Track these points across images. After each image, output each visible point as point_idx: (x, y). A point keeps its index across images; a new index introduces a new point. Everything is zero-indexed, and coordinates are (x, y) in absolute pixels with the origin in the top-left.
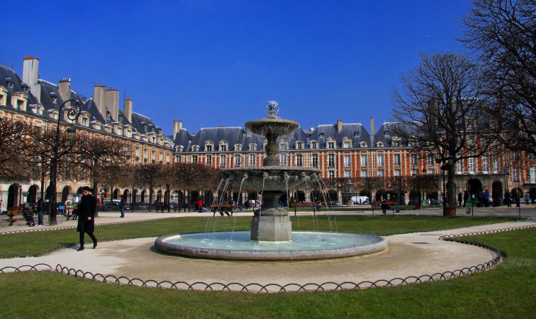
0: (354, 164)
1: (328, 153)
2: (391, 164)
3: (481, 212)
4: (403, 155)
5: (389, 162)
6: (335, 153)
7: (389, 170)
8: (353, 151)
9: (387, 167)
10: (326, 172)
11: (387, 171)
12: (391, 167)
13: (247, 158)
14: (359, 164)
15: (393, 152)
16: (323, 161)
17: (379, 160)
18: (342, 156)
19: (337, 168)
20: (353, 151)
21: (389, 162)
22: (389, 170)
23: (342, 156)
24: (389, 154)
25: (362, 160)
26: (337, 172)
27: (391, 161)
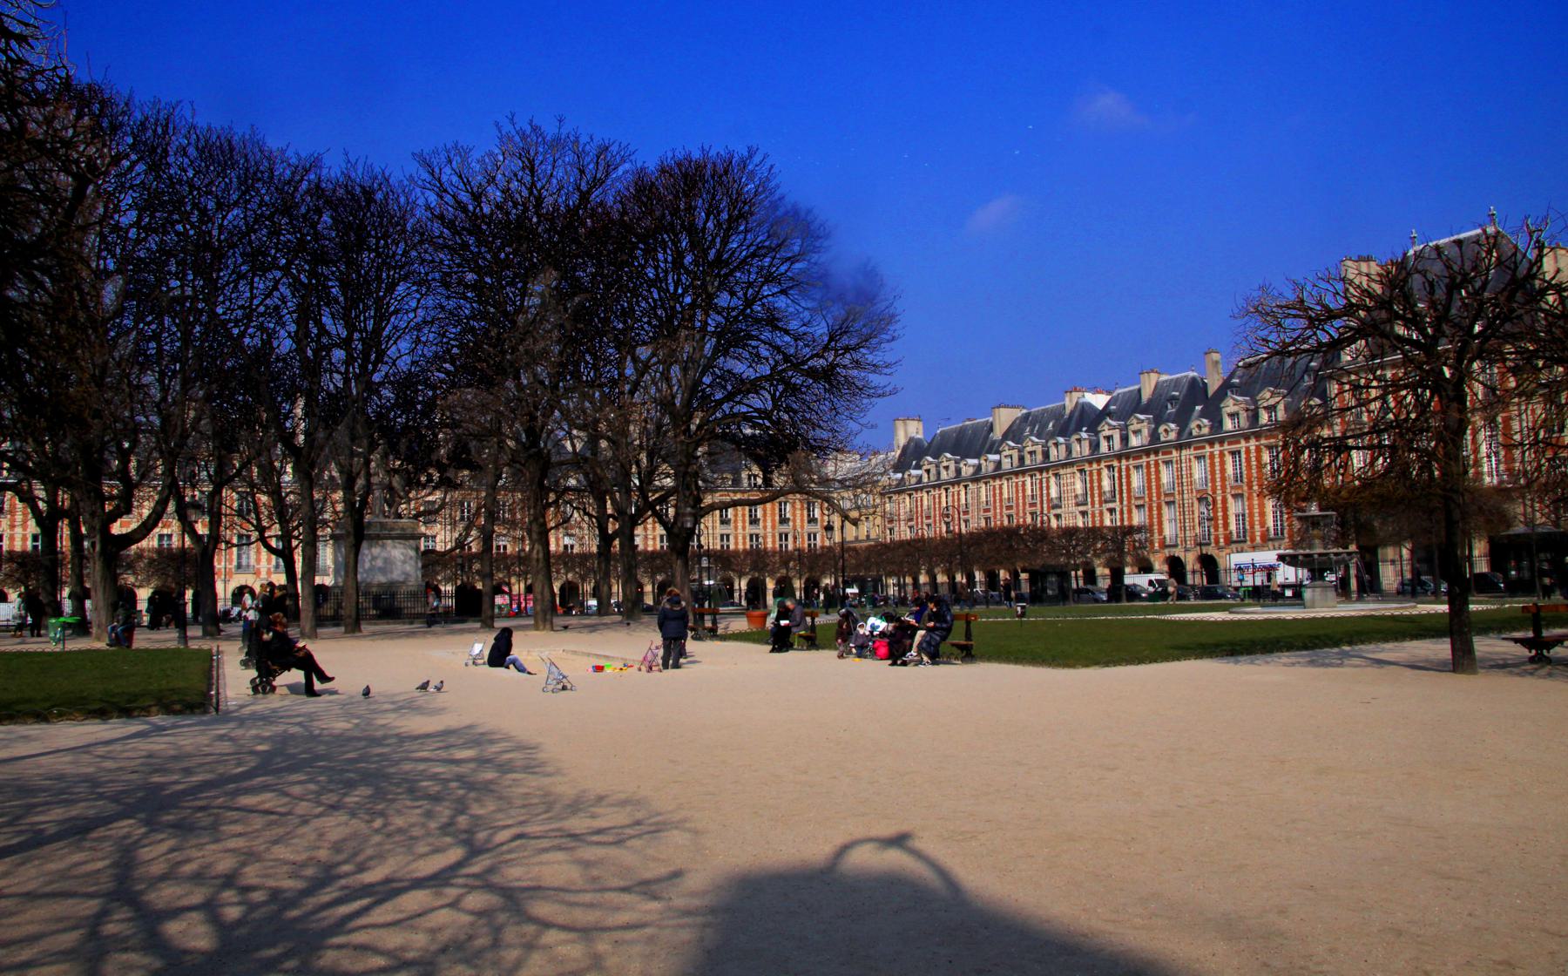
0: (1150, 488)
1: (1103, 465)
2: (1223, 479)
3: (158, 641)
4: (1248, 451)
5: (1218, 476)
6: (1115, 463)
7: (1219, 498)
8: (1247, 439)
9: (1214, 491)
10: (1101, 514)
11: (1214, 501)
12: (1224, 488)
13: (979, 490)
14: (1158, 486)
15: (1226, 446)
17: (1198, 471)
18: (1128, 469)
20: (1247, 439)
21: (1218, 476)
22: (1219, 498)
23: (1128, 469)
24: (1253, 448)
25: (1166, 476)
26: (1122, 513)
27: (1223, 470)
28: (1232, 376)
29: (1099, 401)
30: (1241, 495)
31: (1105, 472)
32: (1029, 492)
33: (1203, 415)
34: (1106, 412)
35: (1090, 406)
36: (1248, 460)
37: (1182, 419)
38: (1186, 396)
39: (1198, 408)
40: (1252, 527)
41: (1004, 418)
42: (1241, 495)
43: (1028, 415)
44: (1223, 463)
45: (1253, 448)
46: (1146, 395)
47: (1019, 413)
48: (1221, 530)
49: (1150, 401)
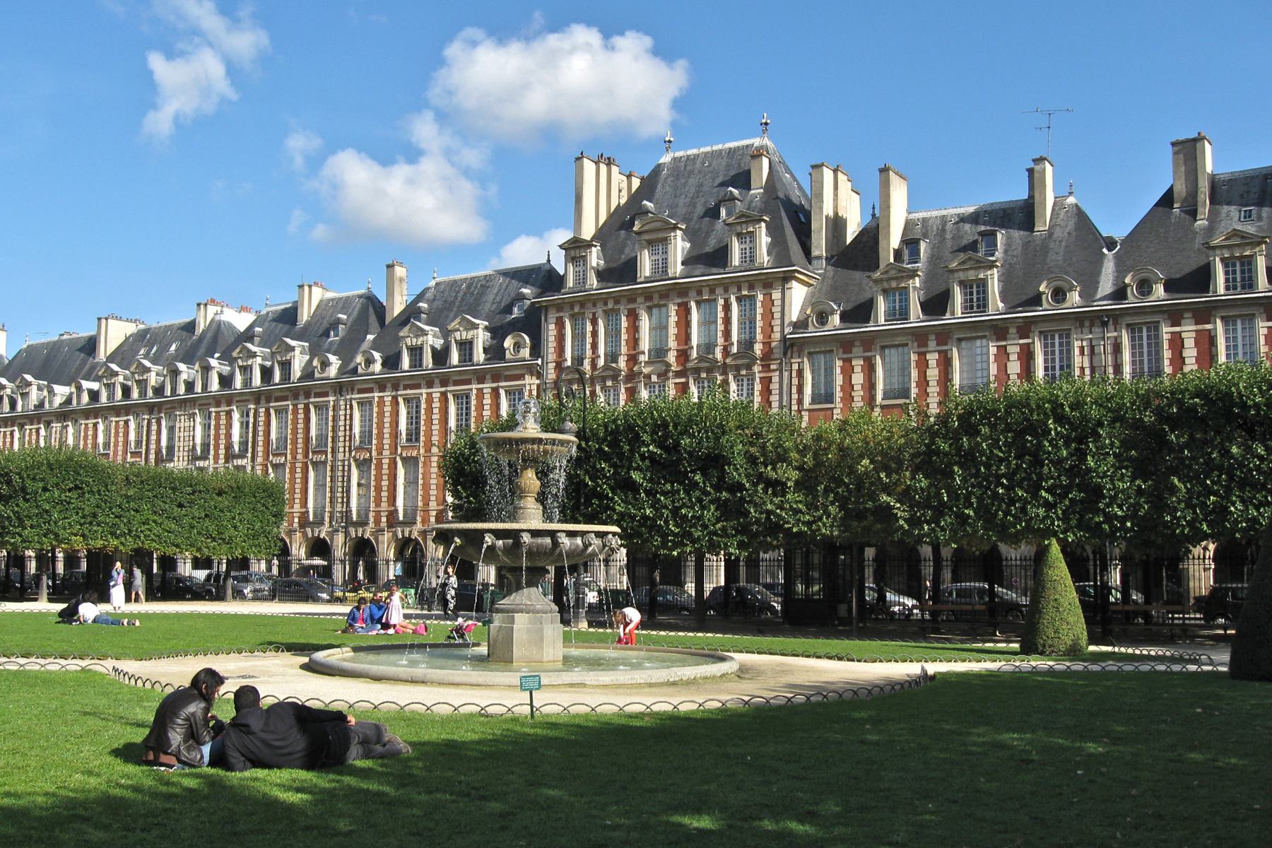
16: (223, 431)
19: (253, 459)
28: (420, 297)
29: (241, 321)
30: (416, 459)
31: (236, 416)
32: (132, 437)
33: (376, 346)
34: (248, 335)
35: (230, 327)
36: (430, 410)
37: (346, 350)
38: (355, 322)
39: (370, 337)
40: (426, 504)
41: (115, 334)
42: (416, 459)
43: (146, 331)
44: (395, 413)
45: (436, 396)
46: (305, 316)
47: (131, 329)
48: (384, 506)
49: (308, 324)
